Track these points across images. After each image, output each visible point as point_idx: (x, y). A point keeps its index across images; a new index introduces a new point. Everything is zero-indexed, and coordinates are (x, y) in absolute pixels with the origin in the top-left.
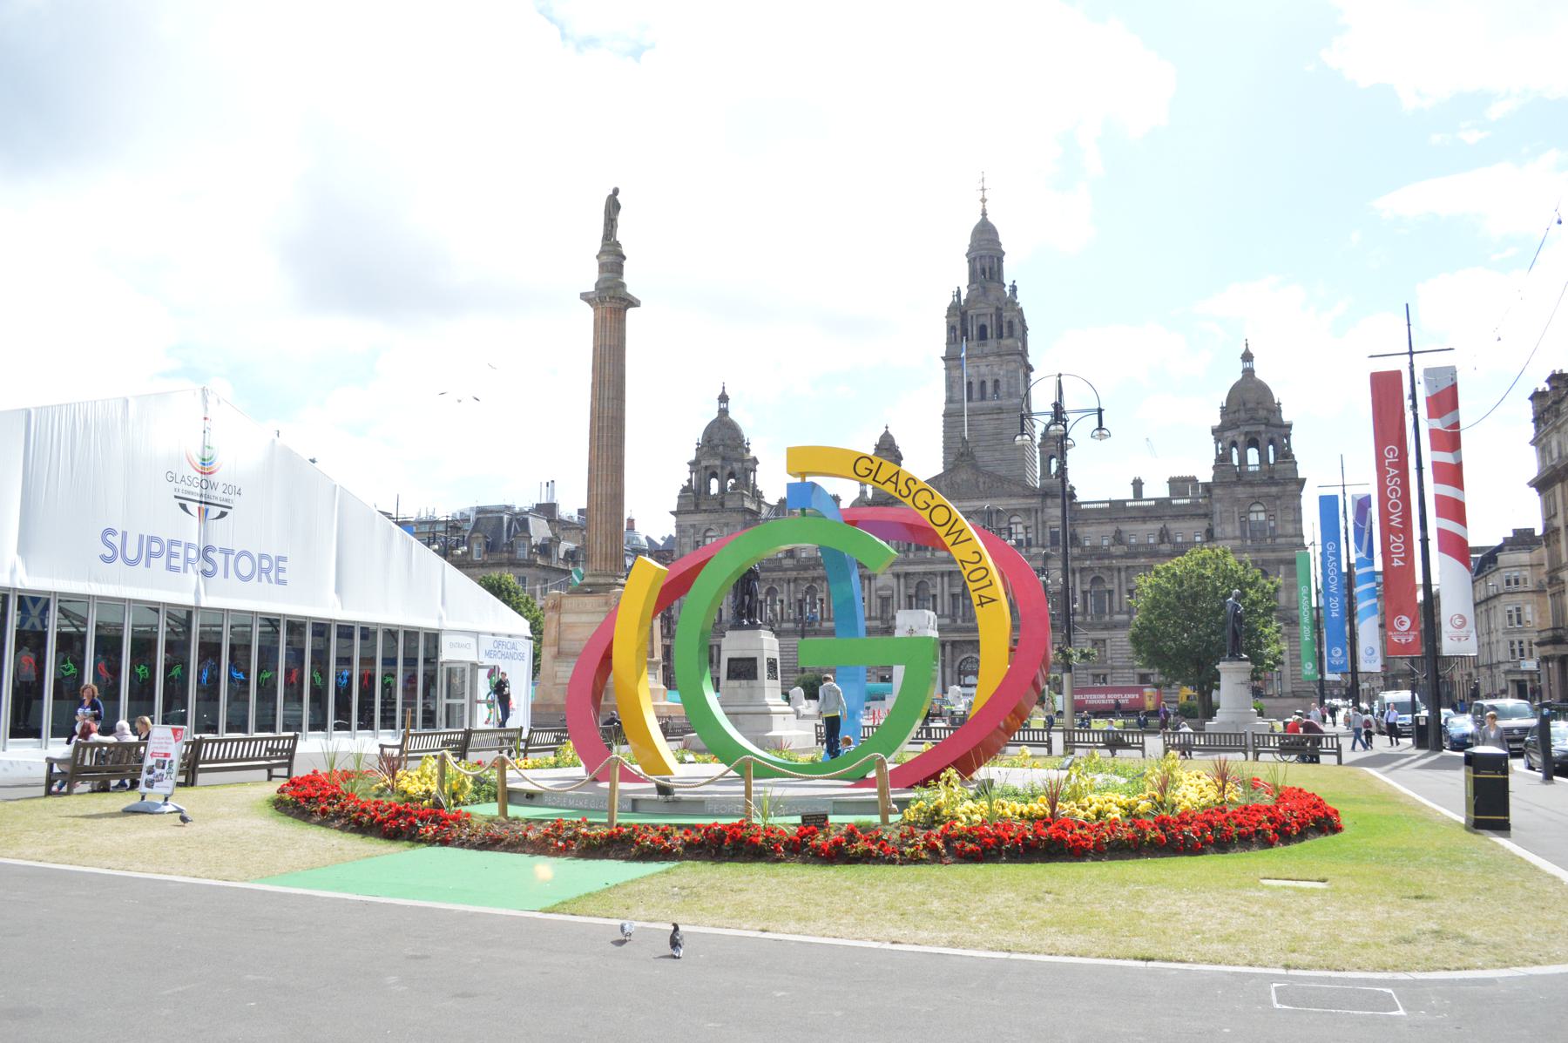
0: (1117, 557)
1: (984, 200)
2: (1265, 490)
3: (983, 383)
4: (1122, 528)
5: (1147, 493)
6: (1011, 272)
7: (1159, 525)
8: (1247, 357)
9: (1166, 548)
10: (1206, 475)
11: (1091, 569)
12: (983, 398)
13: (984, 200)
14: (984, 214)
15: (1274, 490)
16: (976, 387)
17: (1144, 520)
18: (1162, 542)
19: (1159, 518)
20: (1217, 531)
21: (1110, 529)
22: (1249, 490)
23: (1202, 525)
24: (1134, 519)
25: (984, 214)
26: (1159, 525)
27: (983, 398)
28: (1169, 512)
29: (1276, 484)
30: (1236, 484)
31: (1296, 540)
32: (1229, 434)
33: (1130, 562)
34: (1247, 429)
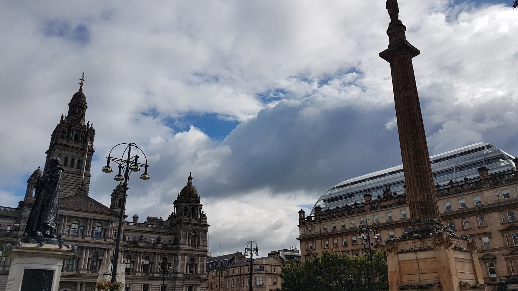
0: (141, 247)
1: (81, 84)
2: (197, 227)
3: (73, 160)
4: (144, 235)
5: (140, 221)
6: (90, 117)
7: (158, 236)
8: (190, 178)
9: (160, 245)
10: (165, 218)
11: (127, 251)
12: (72, 166)
13: (81, 84)
14: (81, 89)
15: (200, 227)
16: (70, 161)
17: (152, 233)
18: (159, 243)
19: (158, 233)
20: (182, 241)
21: (139, 235)
22: (193, 226)
23: (171, 238)
24: (148, 232)
25: (81, 89)
26: (158, 236)
27: (72, 166)
28: (161, 231)
29: (202, 225)
30: (189, 223)
31: (205, 248)
32: (184, 205)
33: (146, 250)
34: (194, 204)
